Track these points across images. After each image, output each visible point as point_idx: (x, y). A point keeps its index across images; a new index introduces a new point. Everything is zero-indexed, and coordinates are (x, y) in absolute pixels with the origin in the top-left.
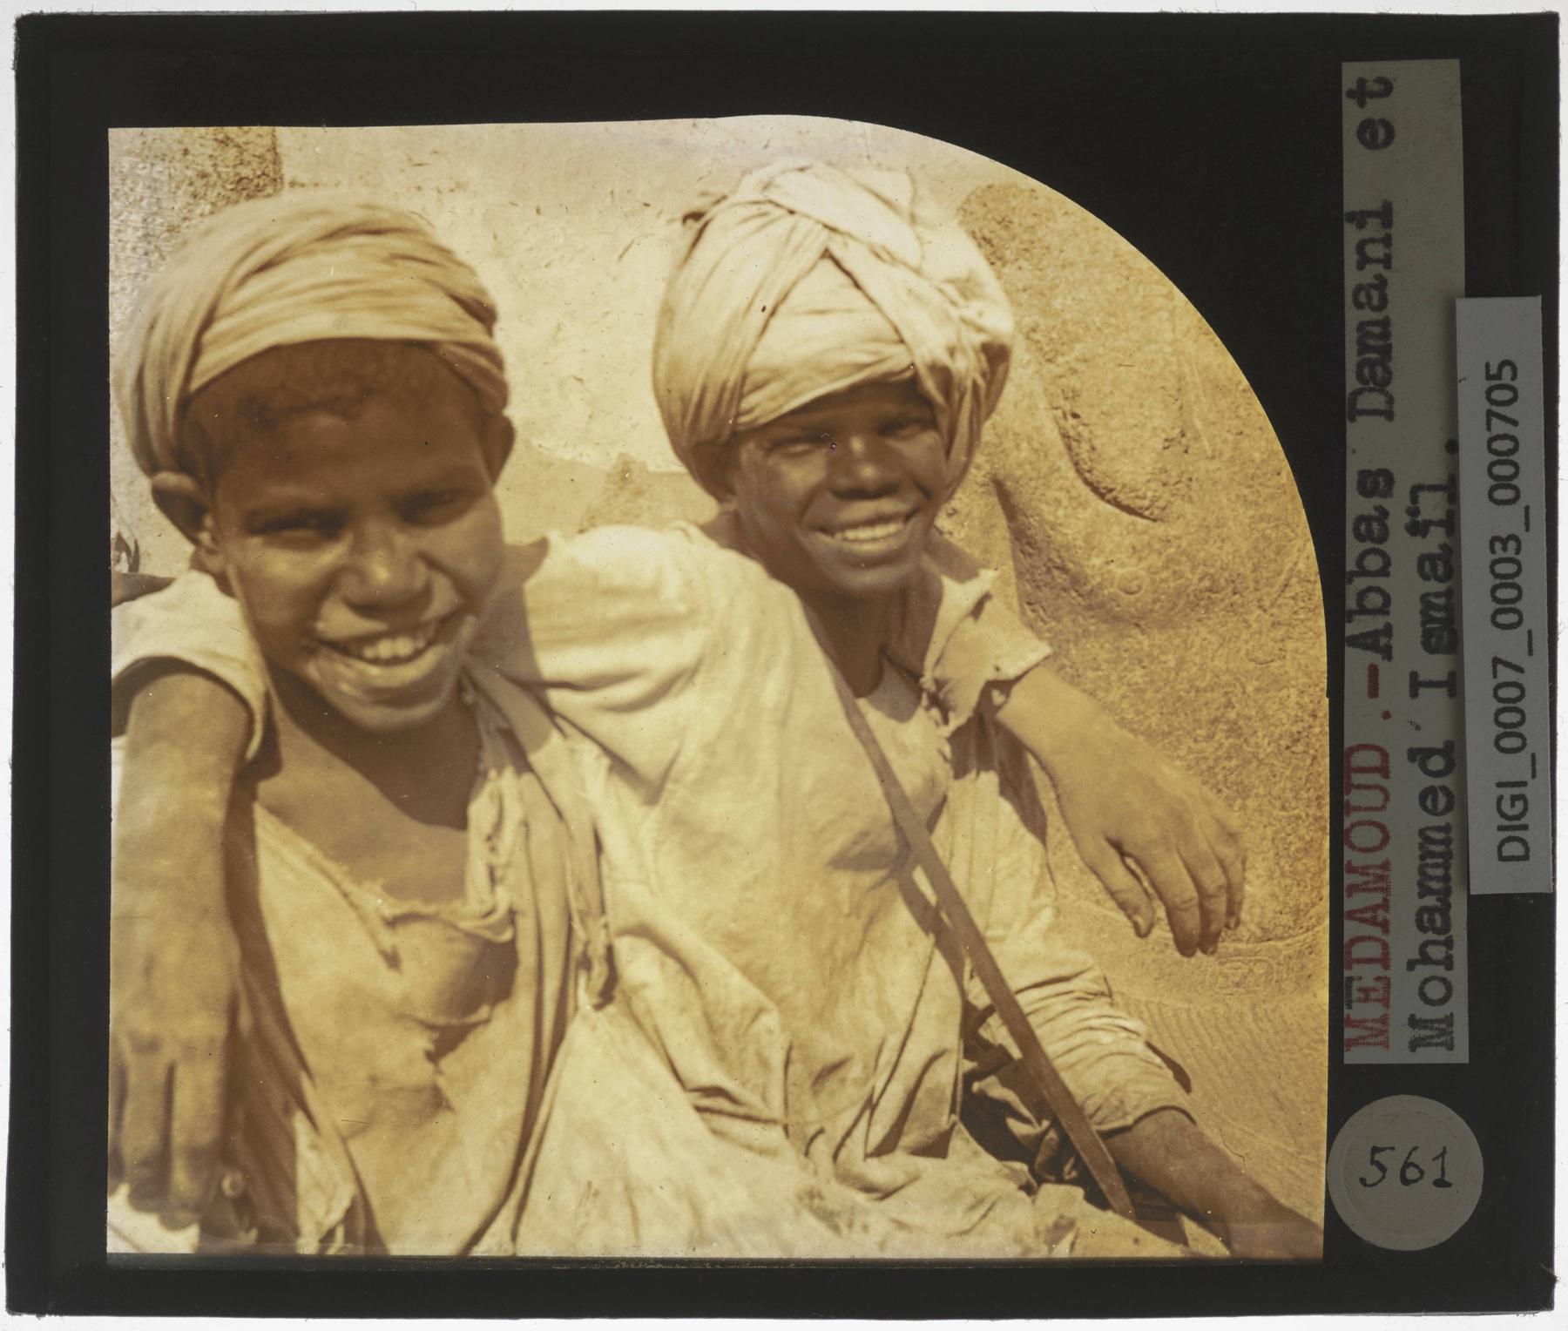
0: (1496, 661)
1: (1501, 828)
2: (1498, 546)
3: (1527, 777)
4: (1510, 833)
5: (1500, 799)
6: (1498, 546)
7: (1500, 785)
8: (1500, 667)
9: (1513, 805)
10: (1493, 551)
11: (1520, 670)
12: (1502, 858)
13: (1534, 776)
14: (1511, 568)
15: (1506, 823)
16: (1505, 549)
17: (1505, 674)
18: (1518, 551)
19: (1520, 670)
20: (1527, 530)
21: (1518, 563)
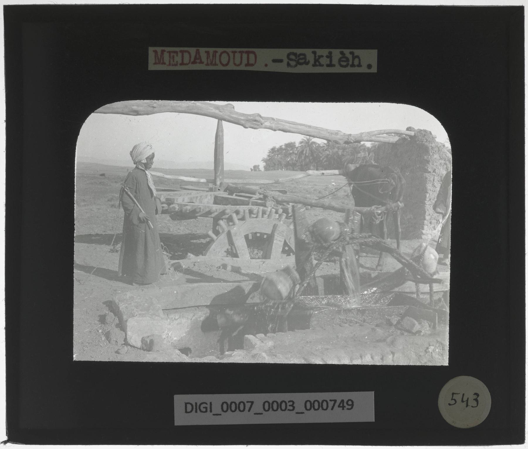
0: (252, 403)
1: (196, 403)
3: (214, 412)
4: (194, 407)
5: (207, 404)
7: (211, 403)
8: (250, 404)
11: (249, 411)
12: (186, 404)
15: (198, 405)
17: (248, 405)
19: (249, 411)
20: (297, 413)
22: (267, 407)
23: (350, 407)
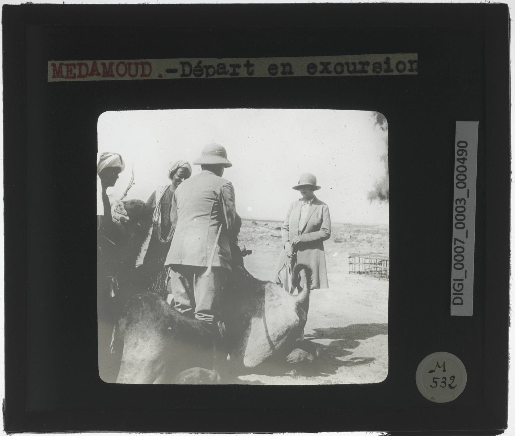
2: (458, 202)
4: (458, 296)
5: (454, 284)
6: (458, 202)
7: (454, 280)
8: (457, 242)
9: (458, 287)
10: (457, 204)
11: (463, 243)
13: (466, 278)
14: (462, 209)
16: (460, 203)
17: (458, 244)
18: (464, 204)
19: (463, 243)
20: (468, 197)
21: (464, 208)
22: (461, 226)
23: (465, 153)
